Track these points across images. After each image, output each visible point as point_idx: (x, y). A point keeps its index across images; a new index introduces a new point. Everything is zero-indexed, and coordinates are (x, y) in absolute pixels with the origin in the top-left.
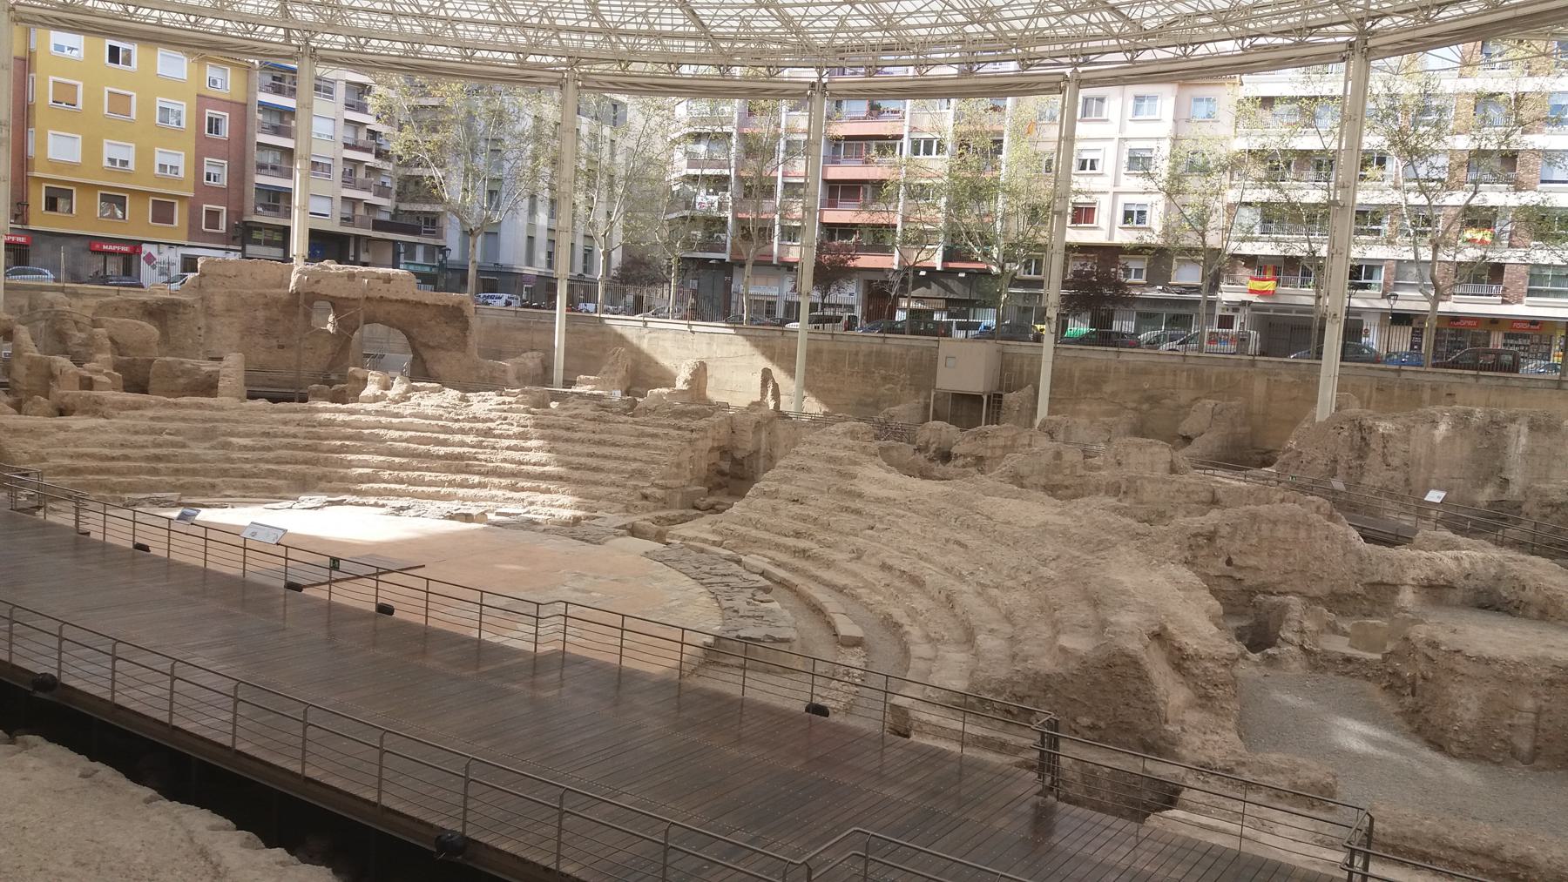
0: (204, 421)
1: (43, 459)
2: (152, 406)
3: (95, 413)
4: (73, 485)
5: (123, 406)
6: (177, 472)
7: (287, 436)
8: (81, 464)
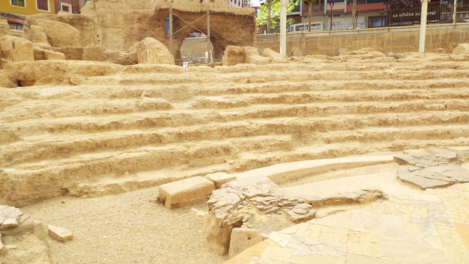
0: (170, 82)
1: (14, 137)
2: (114, 72)
3: (59, 81)
4: (67, 173)
5: (89, 72)
6: (180, 137)
7: (248, 91)
8: (67, 138)
